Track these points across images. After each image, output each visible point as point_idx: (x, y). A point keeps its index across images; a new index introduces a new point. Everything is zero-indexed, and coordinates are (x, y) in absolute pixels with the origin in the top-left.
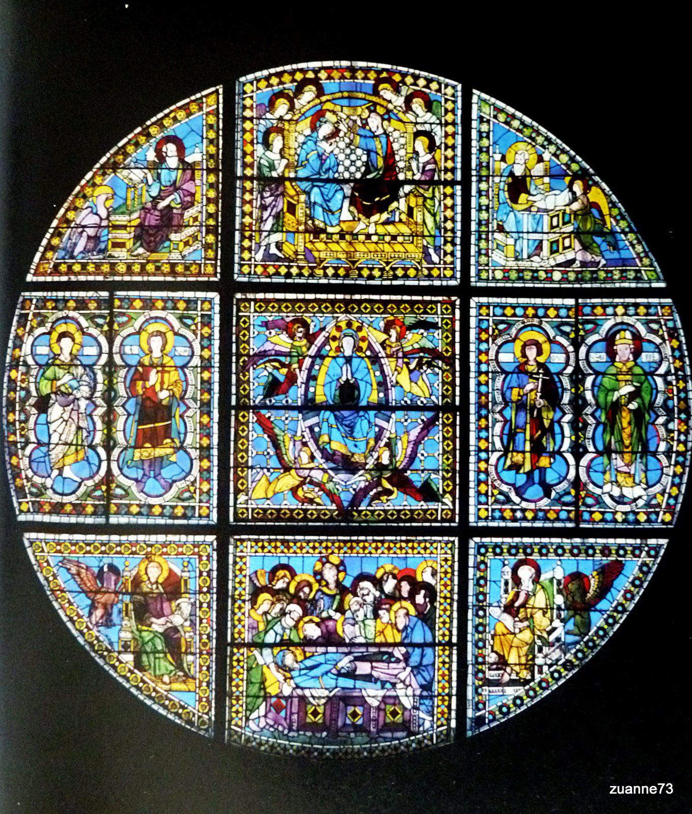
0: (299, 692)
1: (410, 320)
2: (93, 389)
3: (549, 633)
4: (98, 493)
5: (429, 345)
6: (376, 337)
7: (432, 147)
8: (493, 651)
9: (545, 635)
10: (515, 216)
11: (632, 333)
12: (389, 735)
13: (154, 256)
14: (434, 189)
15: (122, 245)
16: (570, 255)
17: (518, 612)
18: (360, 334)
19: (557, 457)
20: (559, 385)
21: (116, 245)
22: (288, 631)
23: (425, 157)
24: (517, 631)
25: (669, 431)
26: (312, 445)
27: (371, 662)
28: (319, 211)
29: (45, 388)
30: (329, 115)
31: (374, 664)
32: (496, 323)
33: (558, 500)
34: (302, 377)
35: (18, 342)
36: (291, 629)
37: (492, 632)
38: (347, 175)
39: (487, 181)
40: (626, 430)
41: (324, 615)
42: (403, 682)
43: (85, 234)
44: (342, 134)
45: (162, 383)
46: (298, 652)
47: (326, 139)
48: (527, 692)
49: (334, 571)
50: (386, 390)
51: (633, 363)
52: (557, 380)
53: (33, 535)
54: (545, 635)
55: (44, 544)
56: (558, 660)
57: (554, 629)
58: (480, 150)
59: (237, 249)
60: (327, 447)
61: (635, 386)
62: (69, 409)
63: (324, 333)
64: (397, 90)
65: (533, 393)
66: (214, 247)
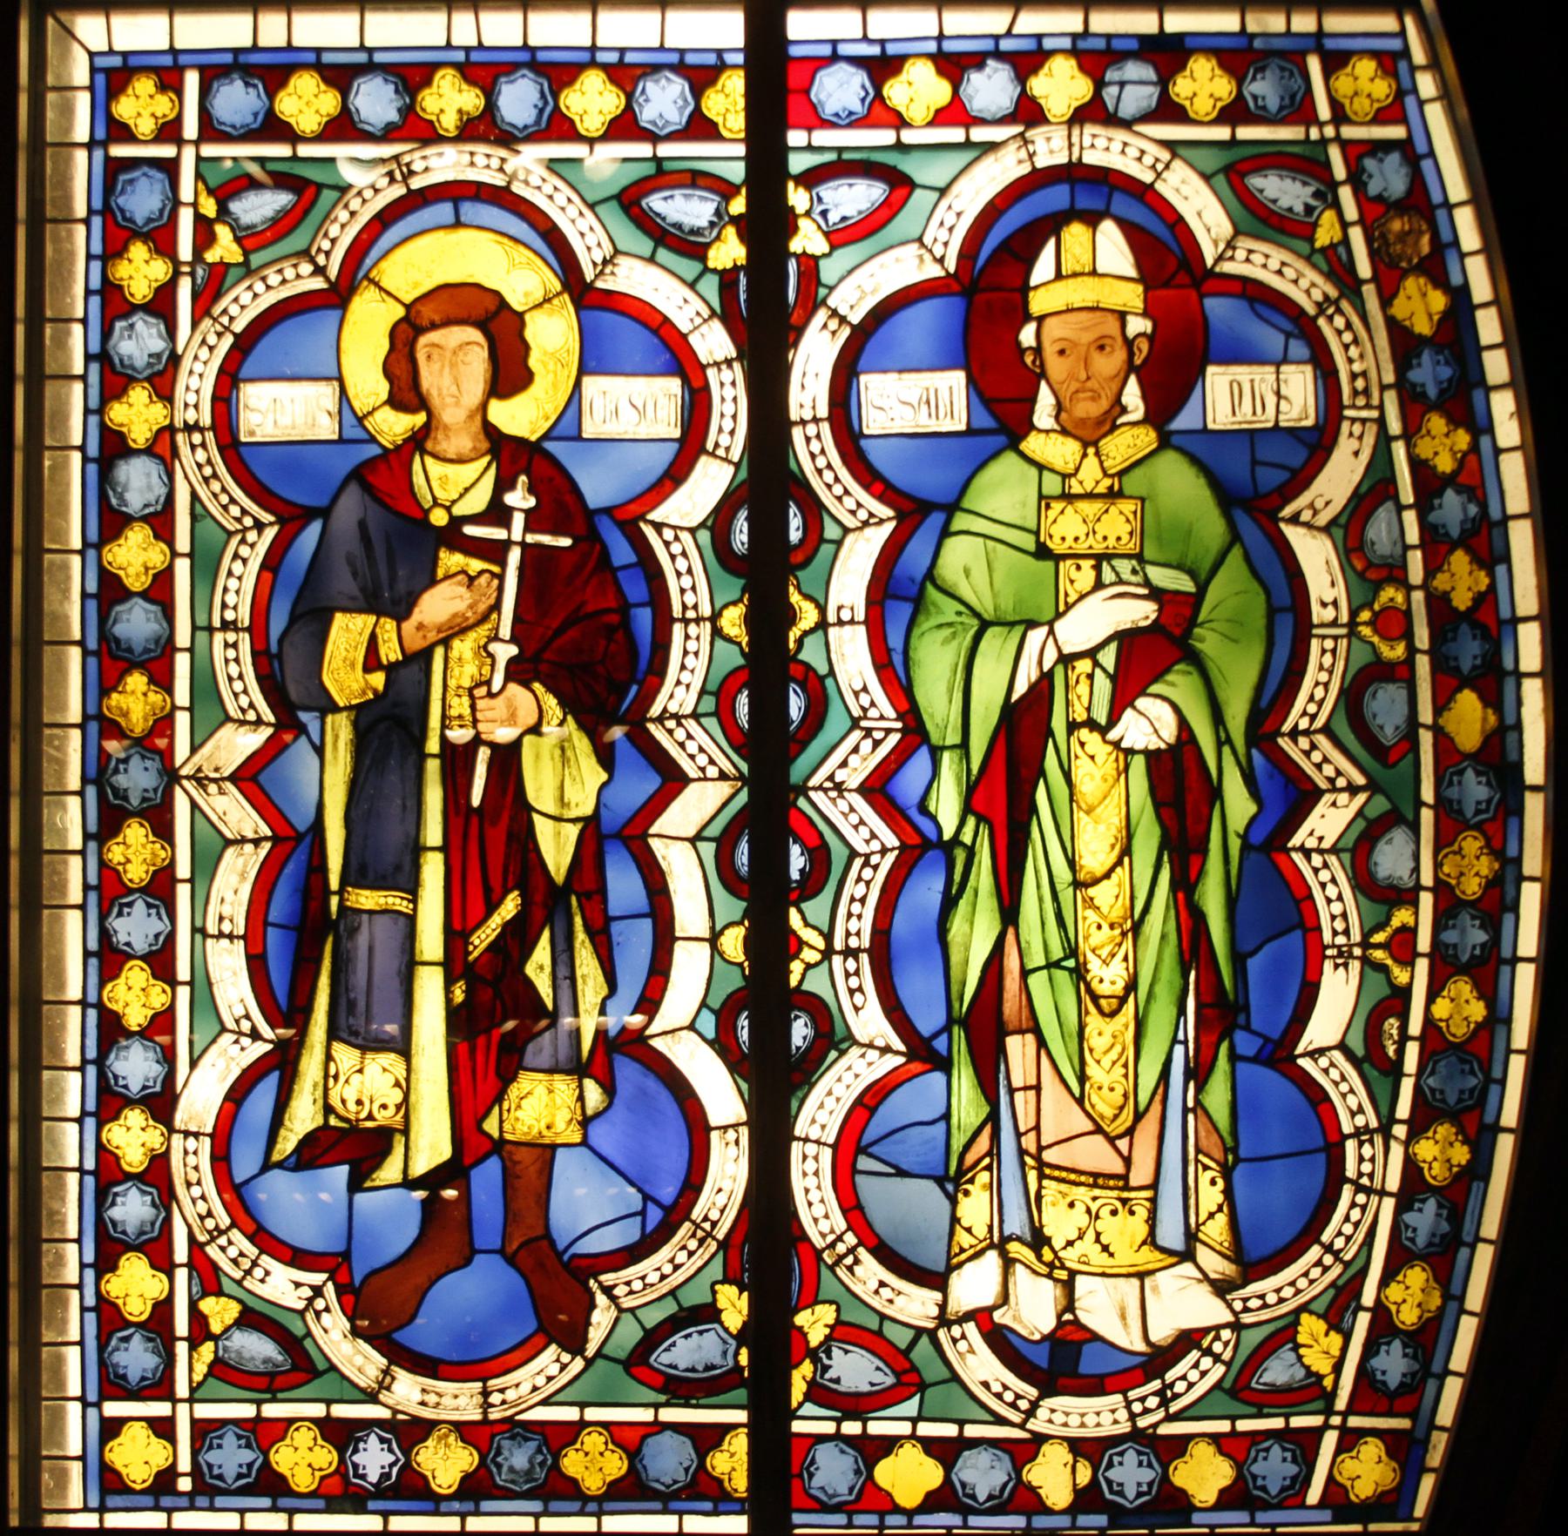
11: (1134, 234)
19: (627, 1071)
20: (635, 589)
40: (1103, 893)
51: (1146, 438)
52: (622, 552)
61: (1156, 594)
65: (463, 647)
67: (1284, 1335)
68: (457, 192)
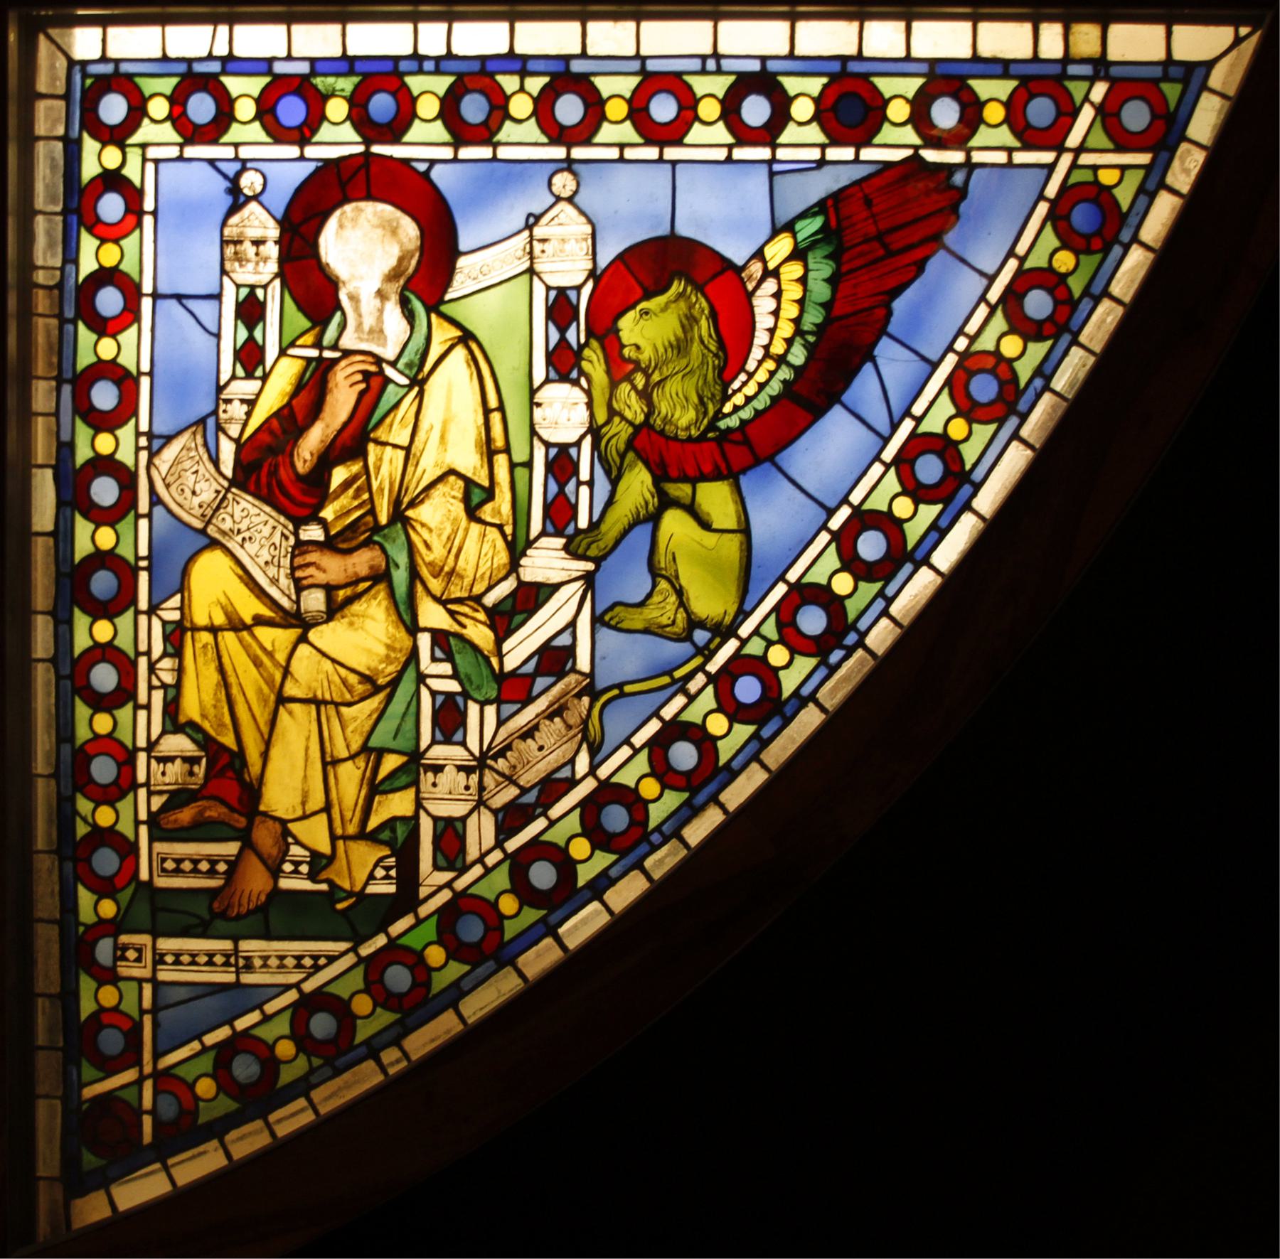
8: (174, 720)
9: (481, 634)
24: (314, 601)
54: (481, 634)
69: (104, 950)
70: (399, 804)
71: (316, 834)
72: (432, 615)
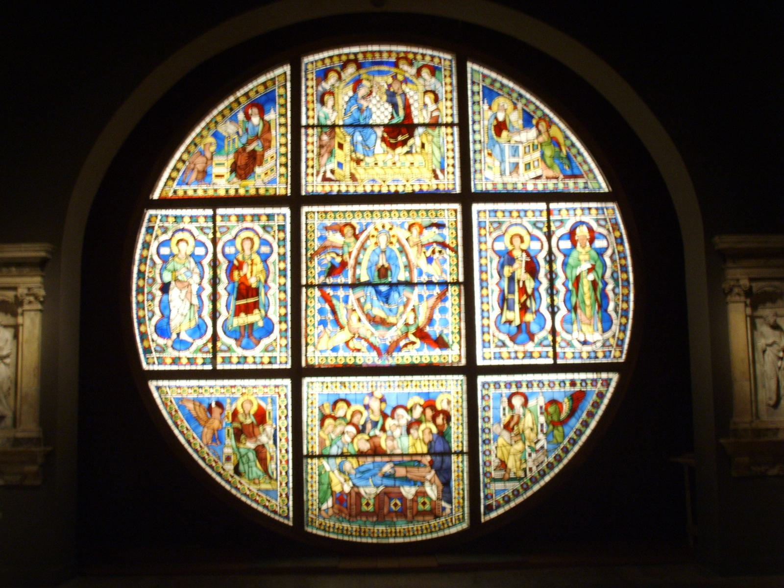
0: (356, 489)
1: (426, 221)
2: (202, 278)
3: (536, 443)
4: (206, 349)
5: (440, 239)
6: (403, 234)
7: (436, 100)
8: (496, 456)
9: (533, 445)
10: (500, 147)
12: (420, 518)
13: (244, 183)
14: (439, 131)
15: (222, 176)
16: (539, 172)
17: (513, 429)
18: (392, 233)
21: (217, 176)
22: (347, 446)
23: (432, 107)
24: (513, 443)
25: (616, 294)
26: (359, 312)
27: (406, 467)
28: (360, 147)
29: (167, 278)
30: (365, 83)
31: (408, 469)
32: (491, 223)
33: (540, 344)
34: (351, 262)
35: (146, 246)
36: (348, 444)
37: (496, 444)
38: (378, 122)
39: (479, 122)
41: (372, 434)
42: (430, 481)
43: (196, 170)
44: (374, 94)
45: (252, 272)
46: (354, 461)
47: (363, 98)
48: (522, 486)
49: (378, 402)
50: (411, 272)
52: (535, 261)
53: (161, 383)
55: (168, 389)
56: (542, 463)
57: (538, 441)
58: (474, 103)
59: (303, 175)
60: (370, 312)
62: (184, 291)
63: (366, 232)
64: (411, 64)
66: (285, 176)
67: (608, 339)
68: (516, 224)
69: (488, 486)
70: (524, 466)
71: (514, 470)
72: (527, 443)
